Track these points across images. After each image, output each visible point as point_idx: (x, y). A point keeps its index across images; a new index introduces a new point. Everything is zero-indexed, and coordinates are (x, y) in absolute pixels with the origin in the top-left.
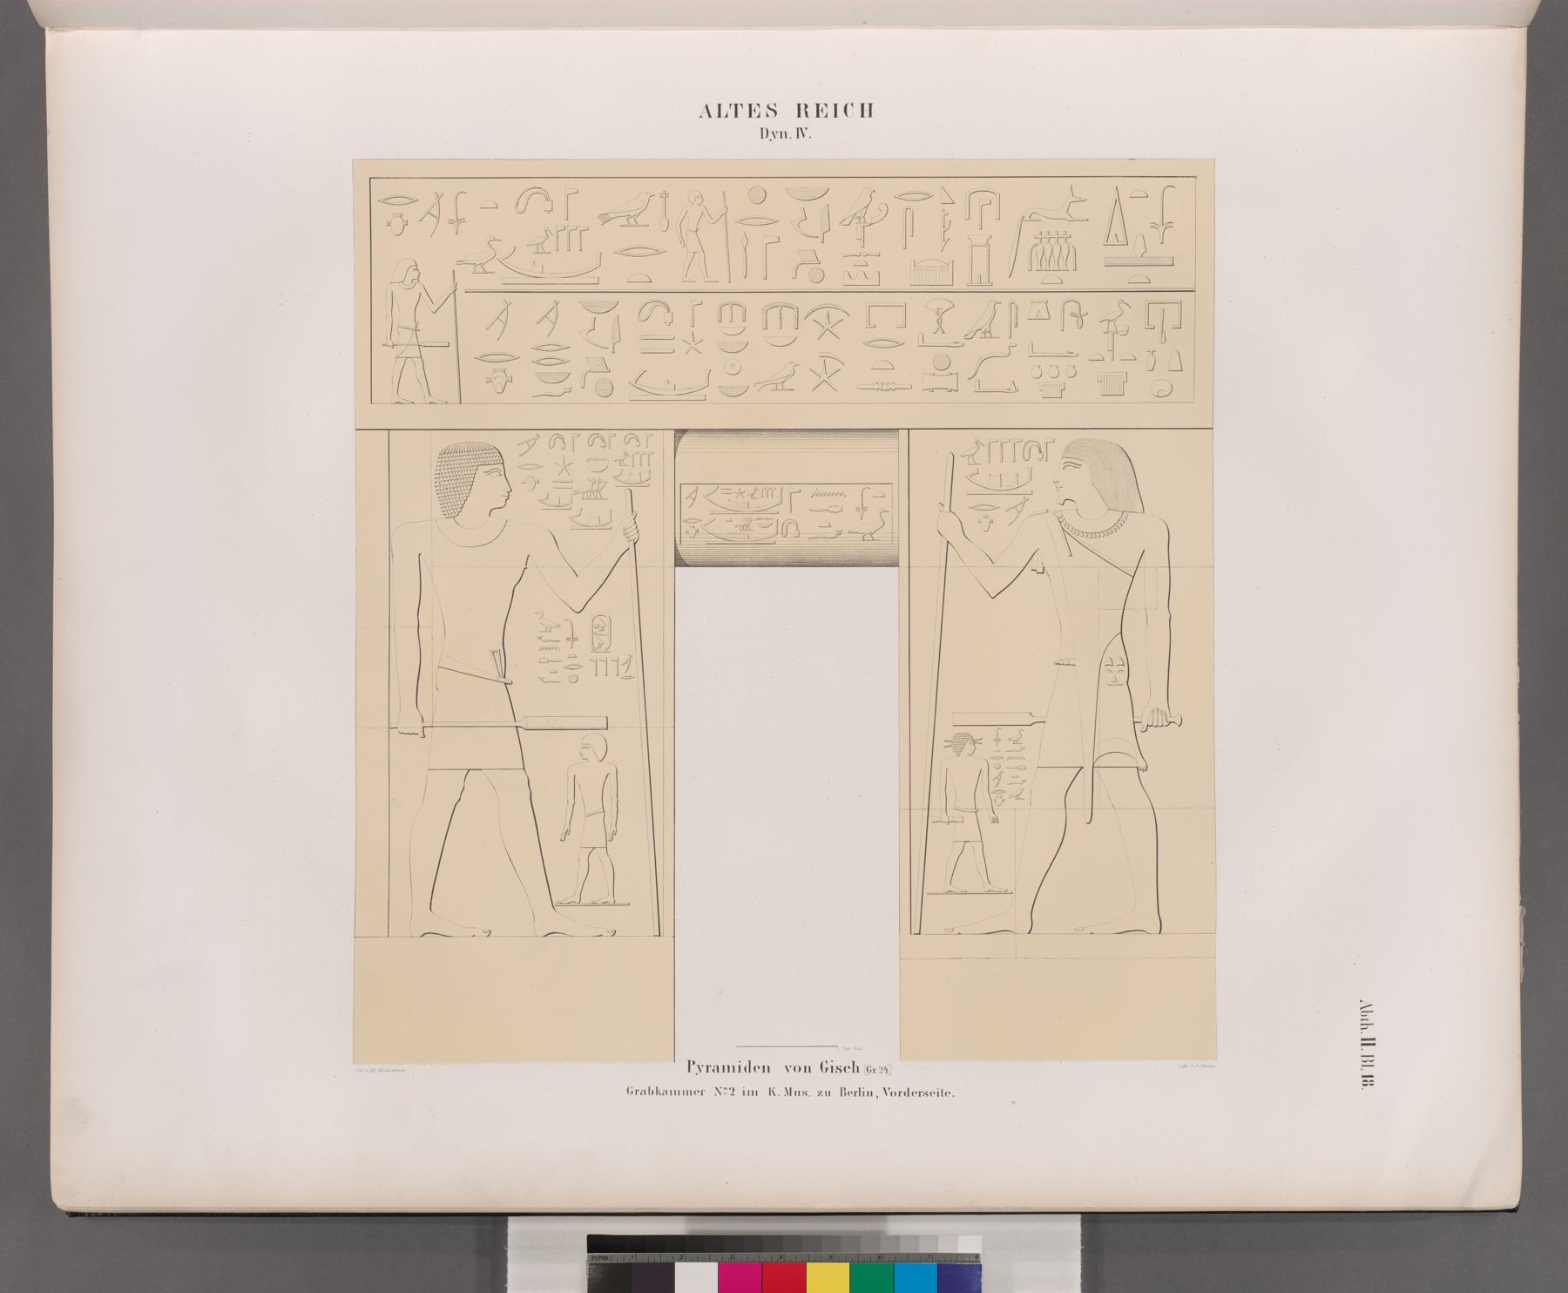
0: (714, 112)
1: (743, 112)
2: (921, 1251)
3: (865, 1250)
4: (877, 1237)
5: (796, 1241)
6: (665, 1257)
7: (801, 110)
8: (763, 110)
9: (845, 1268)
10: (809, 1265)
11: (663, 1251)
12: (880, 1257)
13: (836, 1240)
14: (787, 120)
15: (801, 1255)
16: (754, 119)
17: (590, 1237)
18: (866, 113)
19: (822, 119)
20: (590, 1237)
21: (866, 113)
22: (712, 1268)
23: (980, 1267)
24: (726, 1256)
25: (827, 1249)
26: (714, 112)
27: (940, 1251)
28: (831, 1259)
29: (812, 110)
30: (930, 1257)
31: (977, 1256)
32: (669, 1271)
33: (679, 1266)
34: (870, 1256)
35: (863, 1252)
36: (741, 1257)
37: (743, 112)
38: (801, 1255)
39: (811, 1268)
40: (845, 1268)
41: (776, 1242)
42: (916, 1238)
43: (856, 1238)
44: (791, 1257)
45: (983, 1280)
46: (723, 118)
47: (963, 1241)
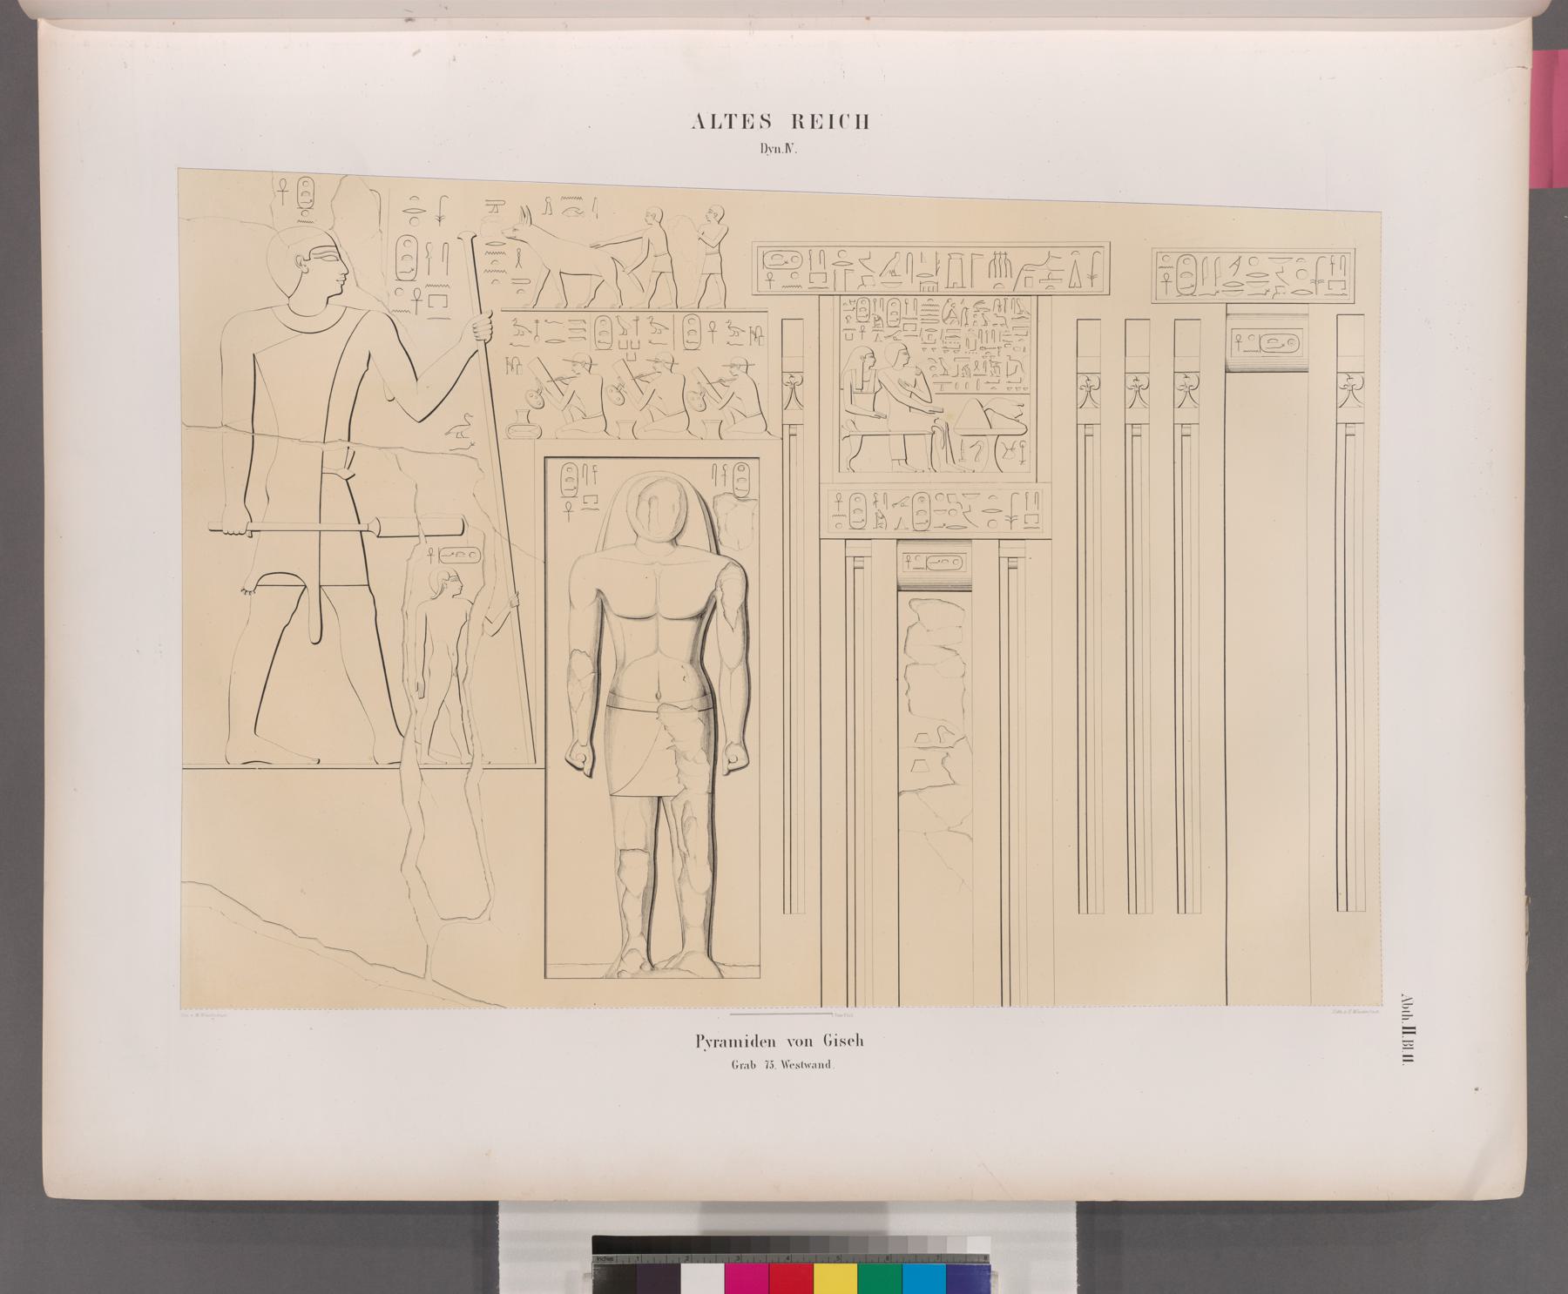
0: (707, 122)
1: (738, 122)
2: (930, 1252)
3: (873, 1250)
4: (883, 1238)
6: (671, 1258)
7: (797, 121)
8: (757, 121)
9: (852, 1269)
10: (817, 1267)
11: (669, 1252)
14: (781, 132)
16: (748, 130)
17: (595, 1238)
18: (862, 125)
19: (816, 130)
20: (595, 1238)
21: (862, 125)
22: (719, 1269)
23: (989, 1267)
24: (733, 1257)
26: (707, 122)
27: (949, 1252)
28: (839, 1260)
29: (807, 122)
30: (939, 1256)
31: (986, 1257)
33: (686, 1269)
34: (879, 1257)
36: (748, 1258)
37: (738, 122)
40: (852, 1269)
43: (863, 1239)
44: (798, 1257)
46: (716, 130)
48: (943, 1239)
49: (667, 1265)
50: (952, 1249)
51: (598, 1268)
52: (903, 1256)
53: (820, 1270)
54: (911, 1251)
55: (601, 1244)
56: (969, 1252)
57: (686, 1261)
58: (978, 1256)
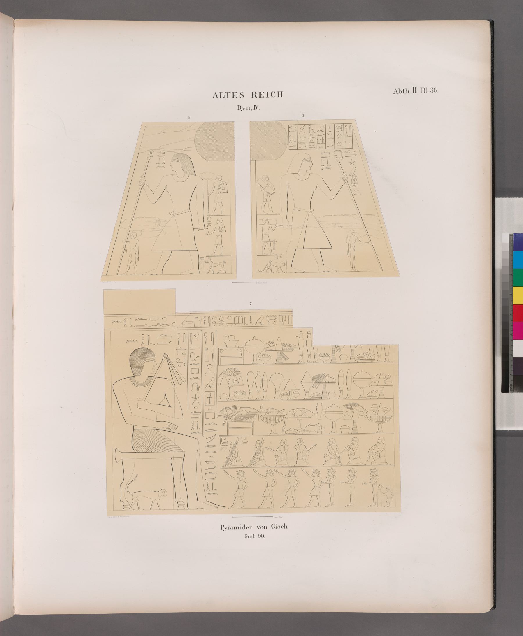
4: (503, 276)
5: (504, 308)
6: (511, 361)
9: (515, 288)
10: (514, 303)
13: (504, 292)
22: (515, 342)
24: (510, 337)
25: (508, 296)
27: (508, 250)
28: (511, 294)
30: (511, 254)
31: (510, 235)
32: (516, 360)
34: (510, 278)
36: (511, 331)
40: (515, 288)
41: (505, 316)
42: (503, 260)
43: (503, 284)
44: (510, 311)
45: (520, 232)
47: (504, 241)
48: (503, 252)
49: (514, 363)
50: (507, 249)
51: (515, 390)
53: (517, 300)
54: (508, 265)
56: (508, 242)
57: (512, 355)
58: (510, 238)
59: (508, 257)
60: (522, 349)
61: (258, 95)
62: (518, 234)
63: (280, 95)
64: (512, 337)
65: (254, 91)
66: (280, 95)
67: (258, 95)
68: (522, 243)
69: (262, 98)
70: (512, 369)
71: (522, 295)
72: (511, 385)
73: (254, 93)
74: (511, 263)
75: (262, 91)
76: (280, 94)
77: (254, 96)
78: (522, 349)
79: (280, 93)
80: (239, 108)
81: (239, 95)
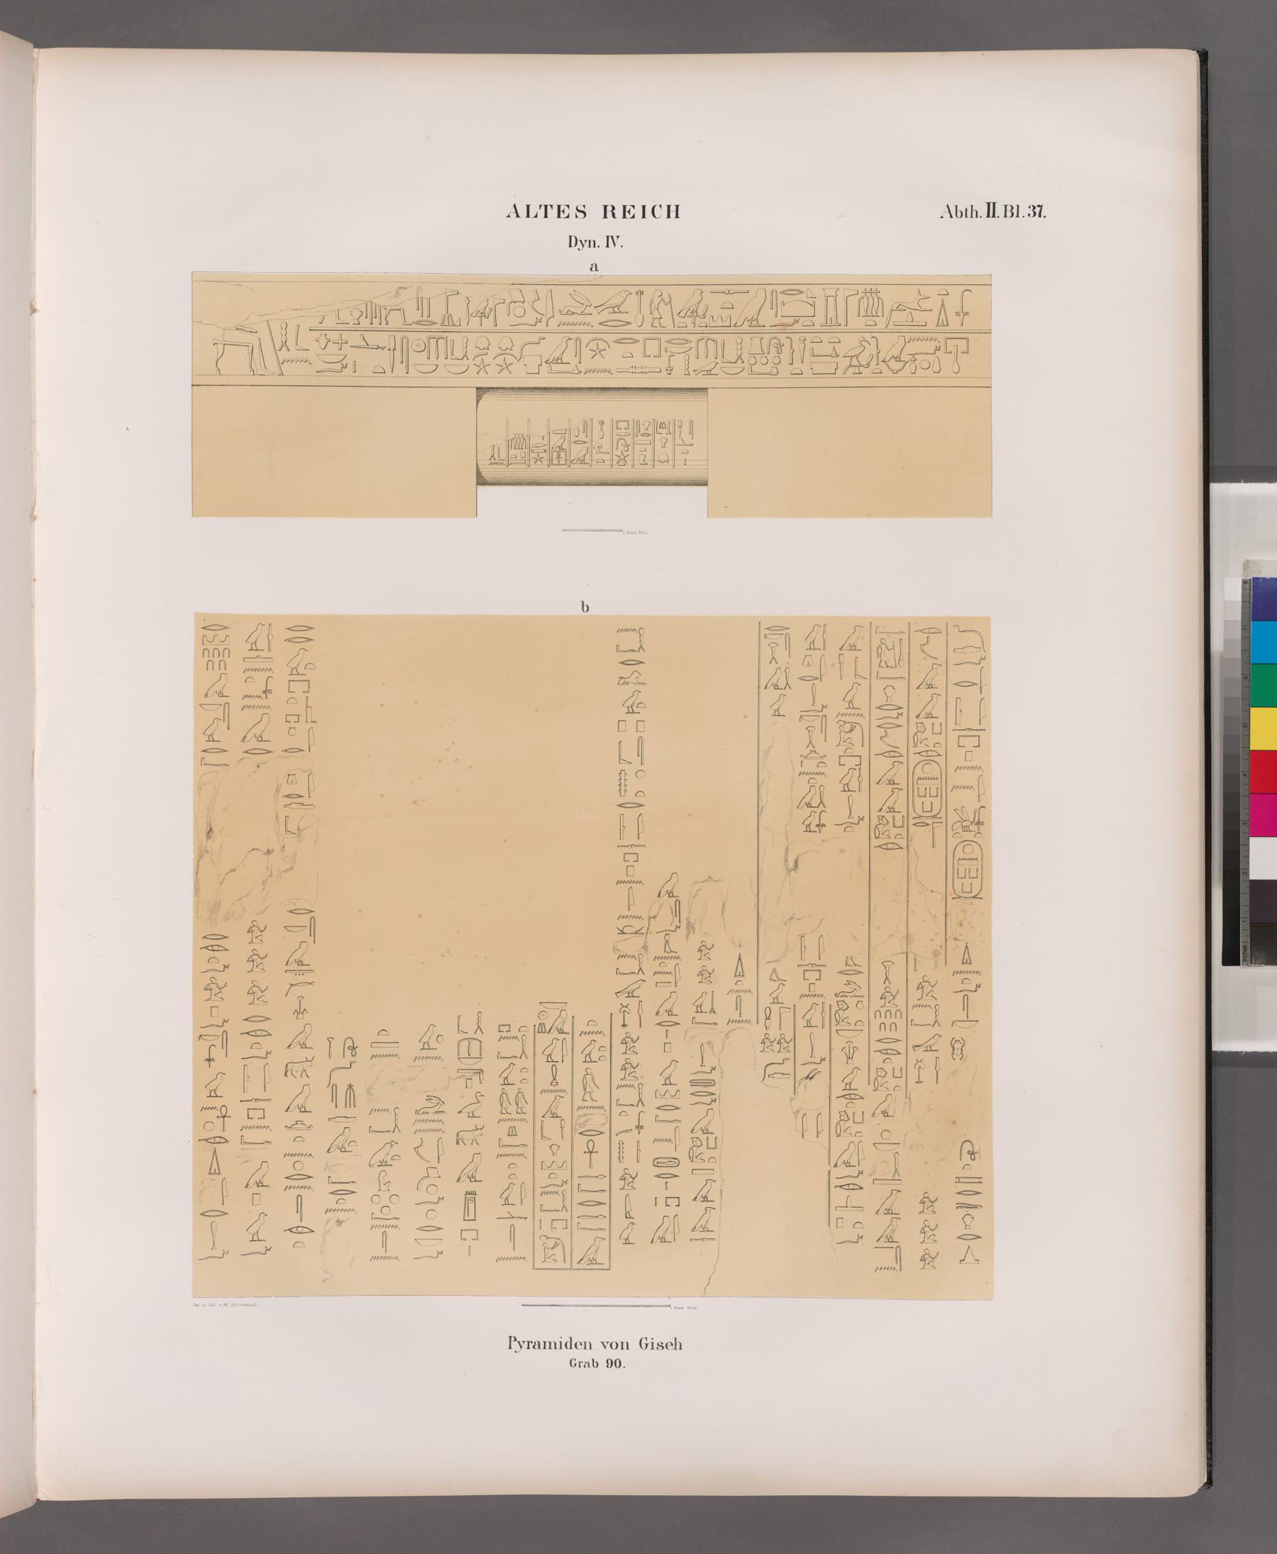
2: (1239, 636)
3: (1238, 692)
4: (1226, 682)
5: (1229, 759)
12: (1245, 677)
13: (1227, 720)
15: (1243, 755)
23: (1256, 579)
24: (1244, 829)
28: (1247, 726)
30: (1243, 629)
33: (1254, 875)
34: (1244, 687)
35: (1240, 695)
36: (1244, 814)
38: (1243, 755)
39: (1256, 745)
42: (1226, 642)
43: (1227, 701)
44: (1244, 766)
45: (1268, 576)
47: (1230, 595)
50: (1237, 615)
51: (1255, 960)
52: (1244, 663)
54: (1239, 655)
55: (1231, 958)
56: (1239, 598)
59: (1237, 635)
60: (1276, 858)
61: (619, 212)
62: (1264, 579)
63: (673, 214)
64: (1247, 830)
65: (609, 203)
66: (673, 214)
67: (619, 212)
68: (1274, 601)
69: (628, 220)
70: (1248, 908)
71: (1276, 729)
72: (1245, 947)
73: (609, 209)
74: (1246, 650)
75: (628, 204)
76: (673, 212)
77: (609, 214)
78: (1276, 858)
79: (673, 209)
80: (573, 241)
81: (572, 211)
